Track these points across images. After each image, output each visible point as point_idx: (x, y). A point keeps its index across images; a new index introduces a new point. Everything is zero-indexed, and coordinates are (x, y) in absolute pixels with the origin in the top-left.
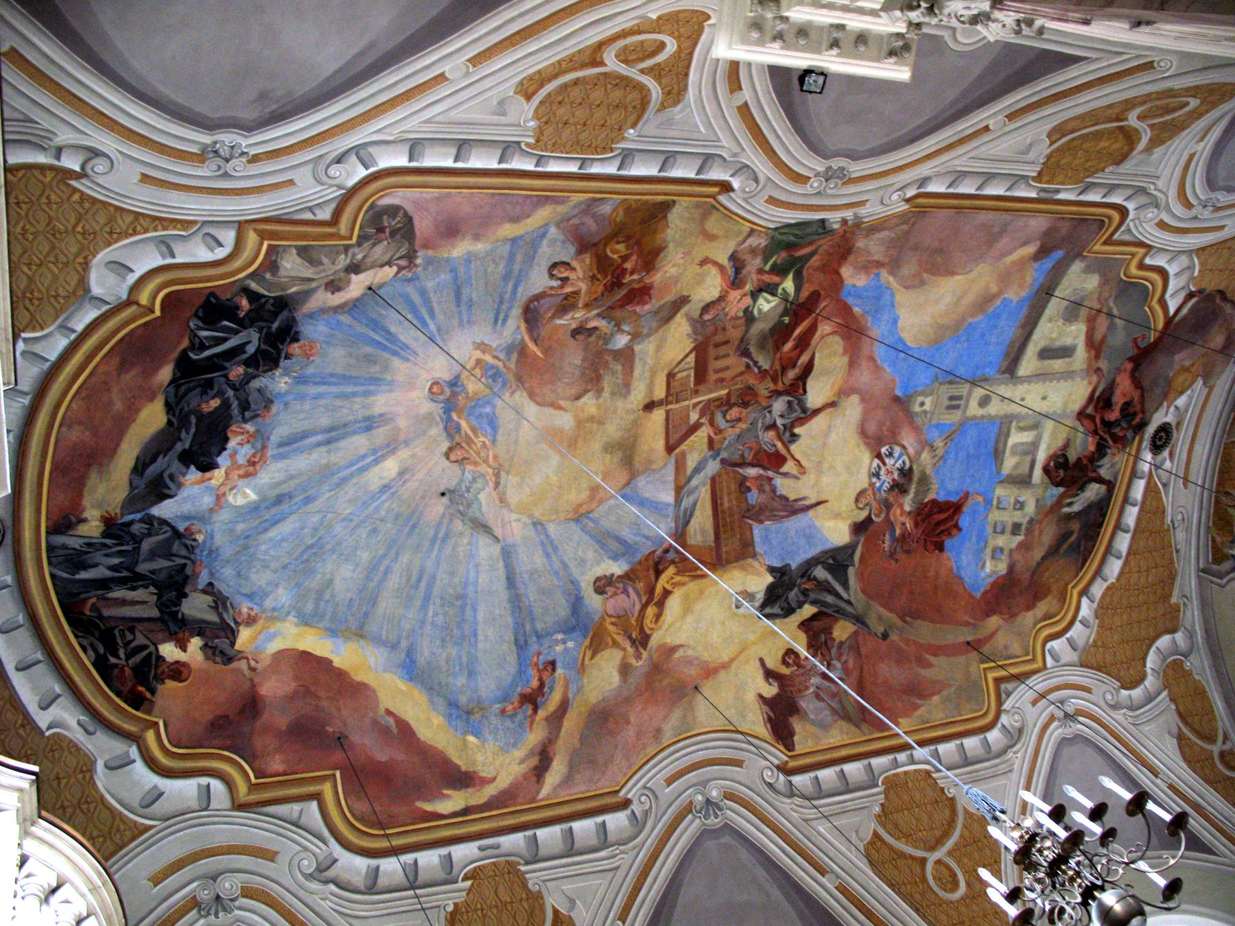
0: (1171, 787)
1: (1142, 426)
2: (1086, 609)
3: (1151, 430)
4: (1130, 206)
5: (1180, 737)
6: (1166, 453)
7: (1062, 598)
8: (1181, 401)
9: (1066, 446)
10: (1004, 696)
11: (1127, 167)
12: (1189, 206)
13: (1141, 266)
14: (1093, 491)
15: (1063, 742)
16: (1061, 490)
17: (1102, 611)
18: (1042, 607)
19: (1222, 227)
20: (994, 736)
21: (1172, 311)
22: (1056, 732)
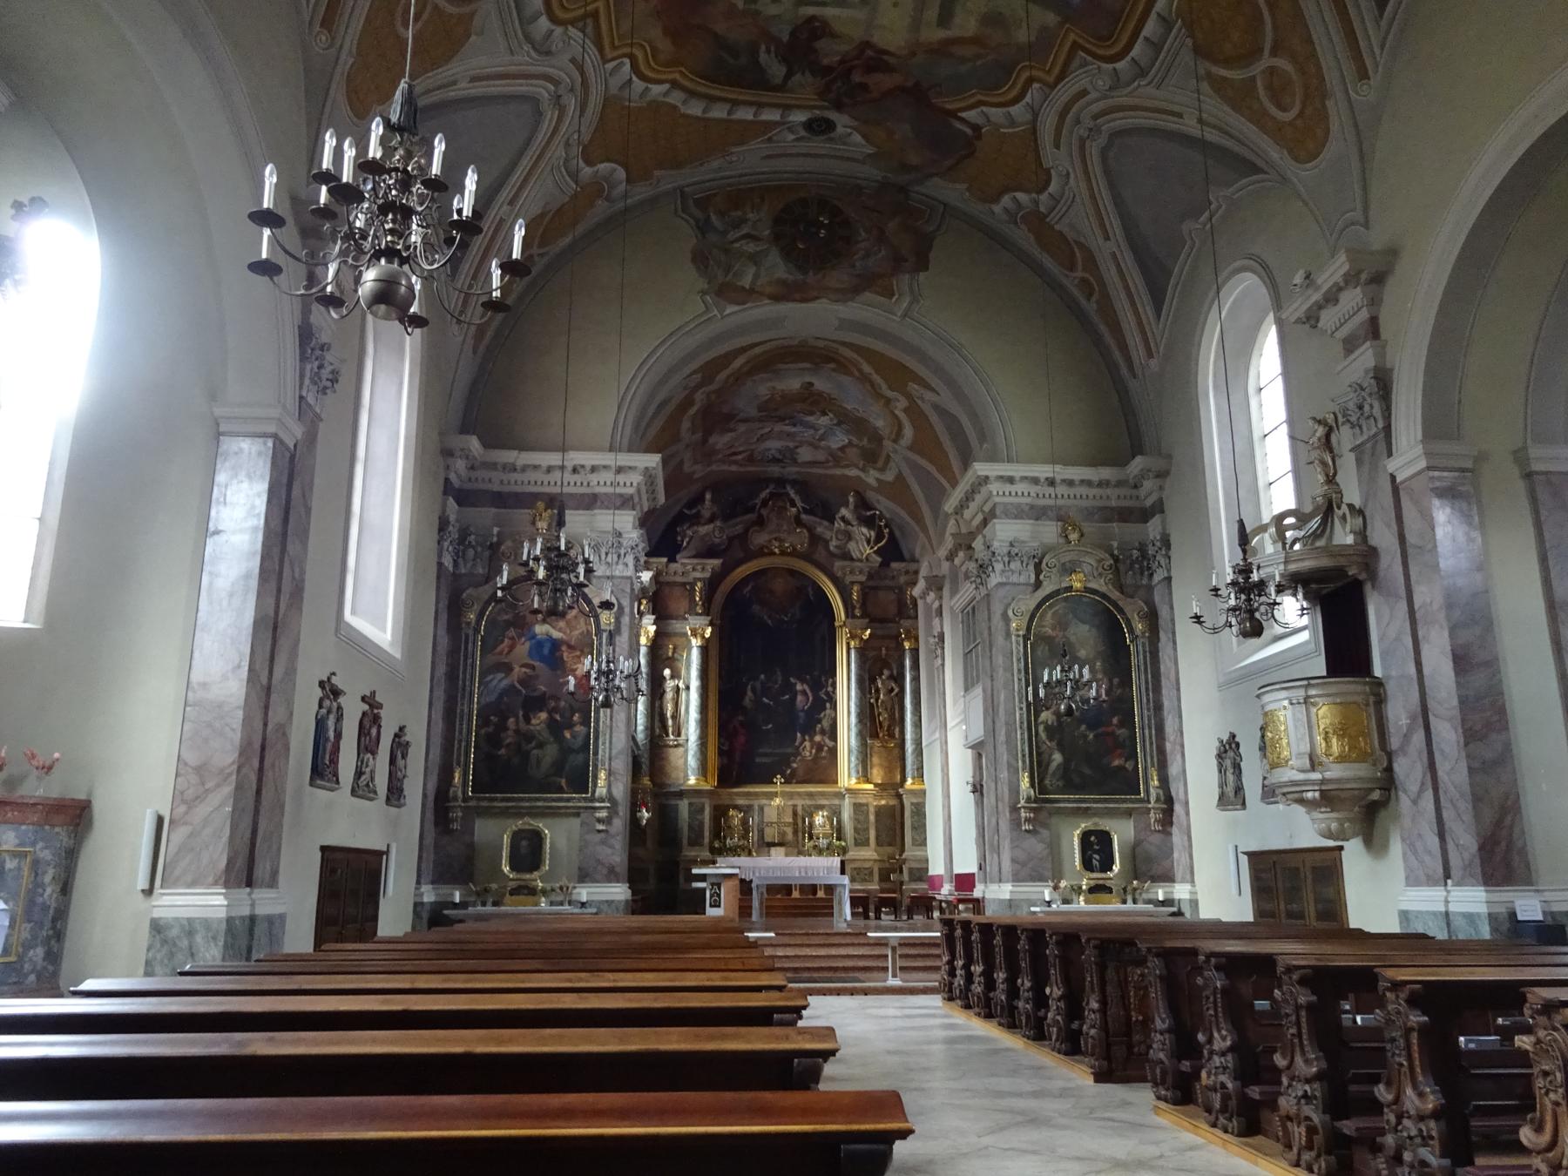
0: (502, 220)
1: (839, 106)
2: (657, 90)
3: (833, 115)
4: (1120, 65)
5: (542, 215)
6: (803, 133)
7: (671, 63)
8: (857, 138)
9: (833, 35)
10: (581, 24)
11: (1187, 57)
12: (1095, 117)
13: (1030, 81)
14: (777, 71)
15: (533, 100)
16: (785, 38)
17: (656, 107)
18: (665, 45)
19: (1057, 147)
20: (544, 23)
21: (963, 115)
22: (543, 91)
